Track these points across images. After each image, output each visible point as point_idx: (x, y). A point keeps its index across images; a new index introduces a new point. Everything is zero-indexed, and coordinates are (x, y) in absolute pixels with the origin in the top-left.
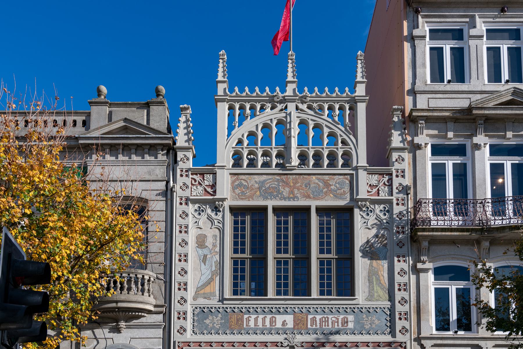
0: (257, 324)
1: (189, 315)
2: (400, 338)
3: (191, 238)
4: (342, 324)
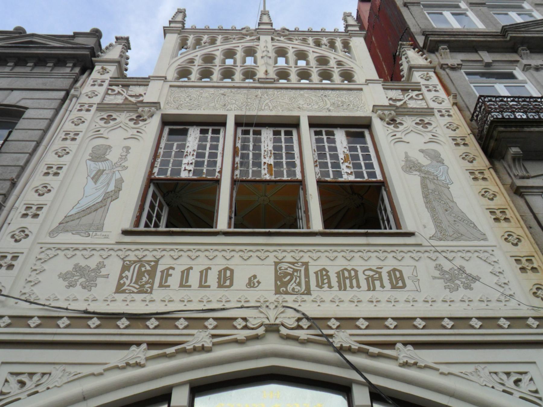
0: (187, 281)
4: (391, 282)
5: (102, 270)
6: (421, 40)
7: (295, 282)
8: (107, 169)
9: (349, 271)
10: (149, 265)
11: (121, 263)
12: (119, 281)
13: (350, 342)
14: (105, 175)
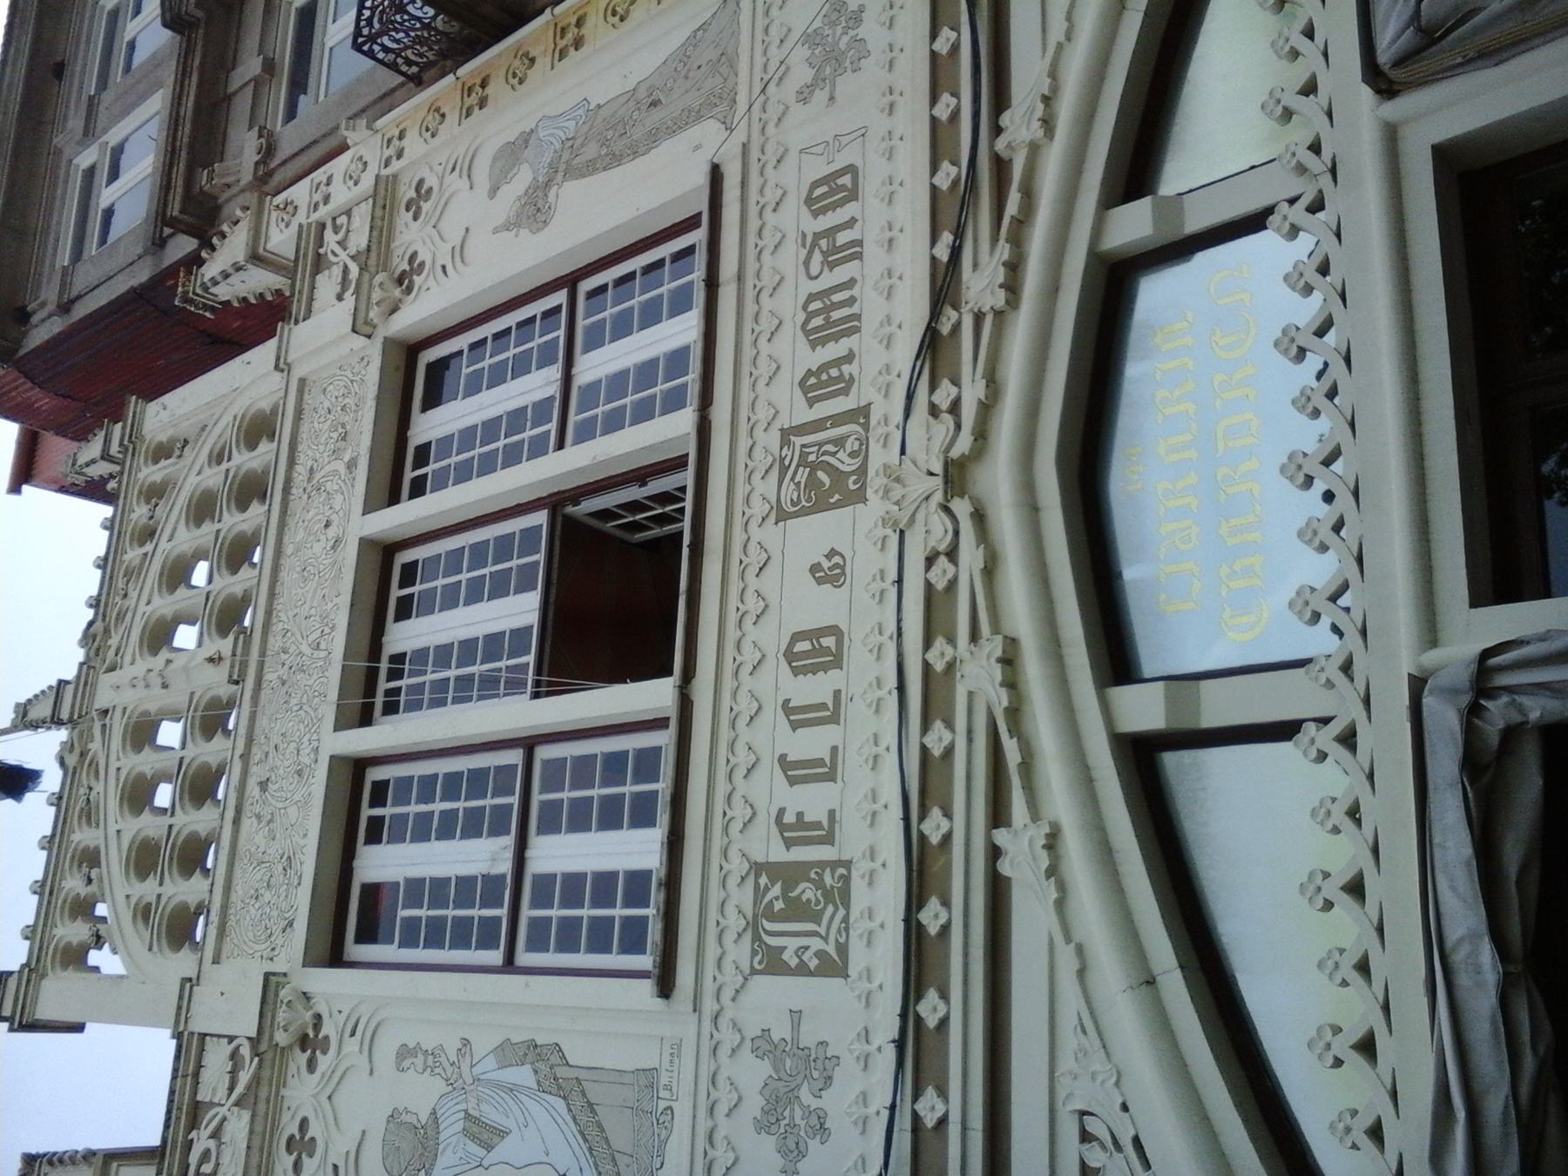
0: (819, 762)
5: (776, 1037)
6: (183, 245)
7: (834, 454)
8: (463, 1106)
9: (811, 316)
10: (767, 889)
11: (758, 980)
12: (811, 974)
13: (993, 264)
14: (484, 1107)
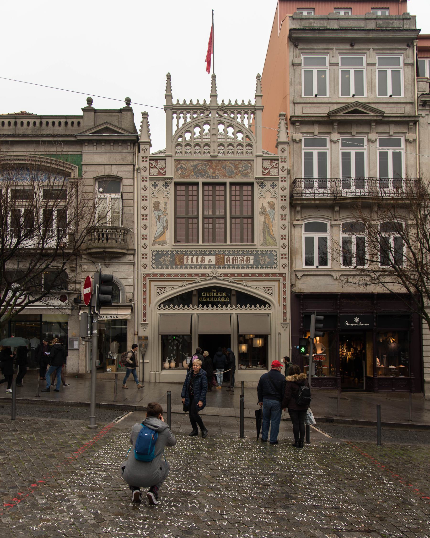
1: (150, 256)
2: (282, 271)
3: (150, 204)
